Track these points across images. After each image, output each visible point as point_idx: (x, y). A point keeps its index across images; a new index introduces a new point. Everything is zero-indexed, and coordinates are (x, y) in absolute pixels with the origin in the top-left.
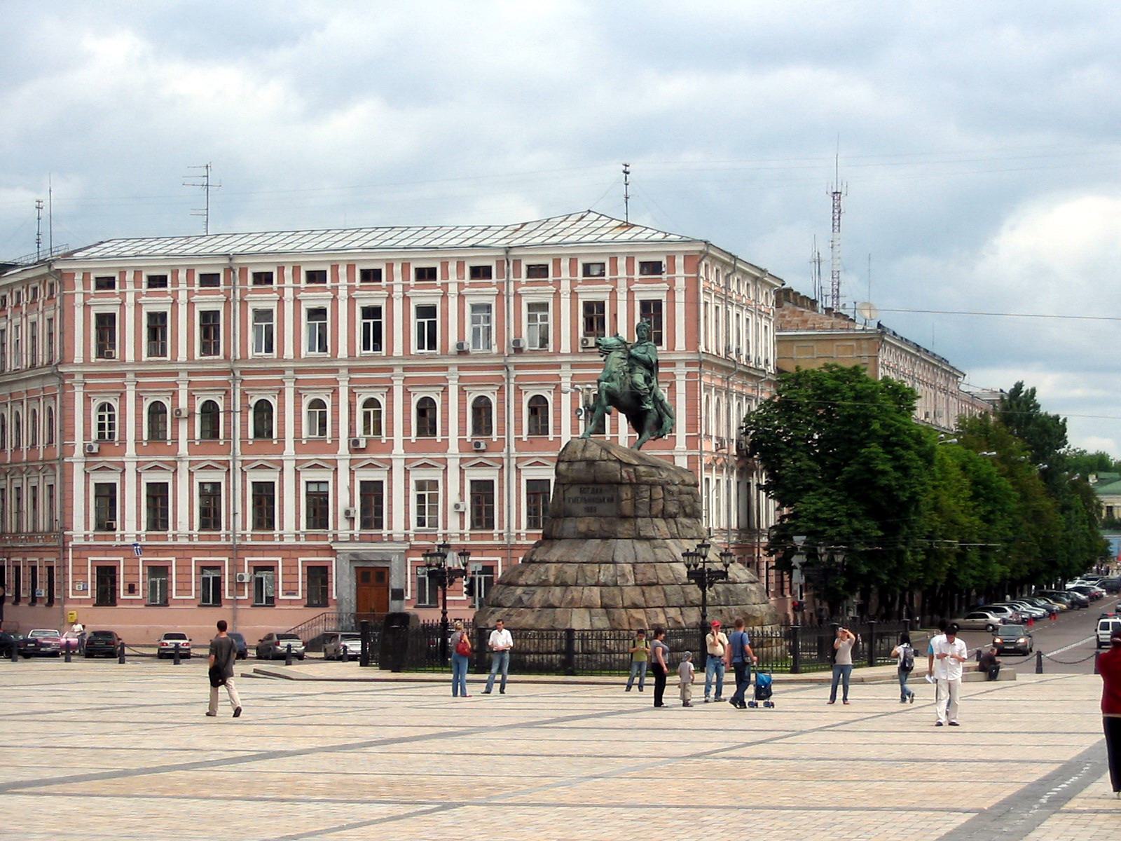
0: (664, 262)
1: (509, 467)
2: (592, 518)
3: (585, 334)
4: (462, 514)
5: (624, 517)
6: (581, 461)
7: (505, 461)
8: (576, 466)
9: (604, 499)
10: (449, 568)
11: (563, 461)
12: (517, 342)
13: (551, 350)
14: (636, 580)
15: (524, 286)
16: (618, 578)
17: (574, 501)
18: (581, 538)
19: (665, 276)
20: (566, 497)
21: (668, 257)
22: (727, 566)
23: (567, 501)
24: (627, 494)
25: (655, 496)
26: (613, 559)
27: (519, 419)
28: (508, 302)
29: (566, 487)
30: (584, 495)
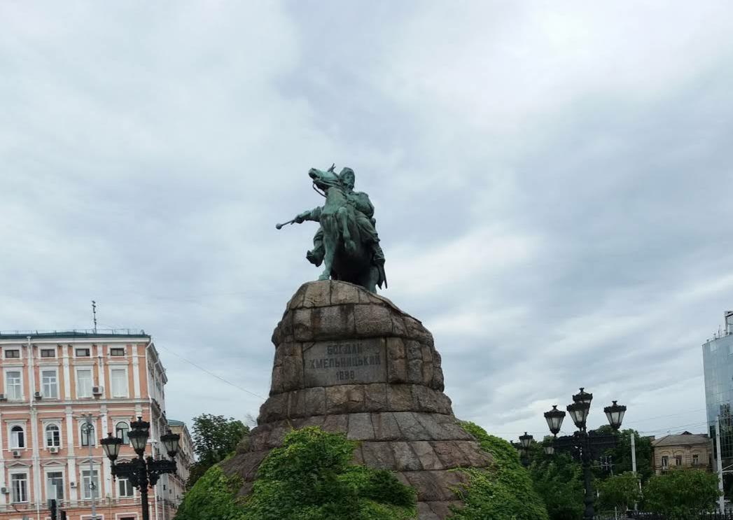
0: (125, 349)
2: (354, 386)
4: (7, 494)
5: (397, 383)
6: (331, 305)
8: (326, 313)
9: (365, 359)
10: (150, 459)
11: (301, 308)
12: (37, 393)
14: (443, 462)
16: (422, 460)
17: (319, 366)
18: (339, 413)
19: (126, 356)
21: (127, 346)
24: (400, 350)
30: (334, 356)
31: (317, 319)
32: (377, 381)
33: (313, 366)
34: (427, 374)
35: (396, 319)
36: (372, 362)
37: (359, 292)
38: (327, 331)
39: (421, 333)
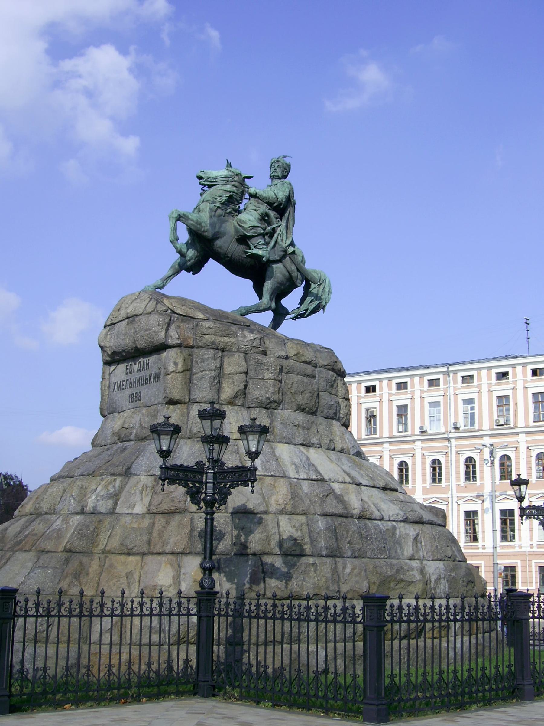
1: (452, 503)
2: (133, 410)
3: (498, 416)
7: (450, 499)
9: (150, 377)
12: (455, 424)
13: (477, 427)
15: (460, 389)
20: (112, 385)
22: (254, 456)
23: (112, 388)
24: (176, 364)
25: (228, 369)
26: (129, 468)
27: (458, 473)
28: (450, 399)
29: (113, 368)
31: (109, 337)
32: (156, 402)
33: (114, 389)
34: (227, 389)
35: (179, 327)
36: (155, 378)
37: (151, 299)
38: (115, 349)
39: (219, 339)
